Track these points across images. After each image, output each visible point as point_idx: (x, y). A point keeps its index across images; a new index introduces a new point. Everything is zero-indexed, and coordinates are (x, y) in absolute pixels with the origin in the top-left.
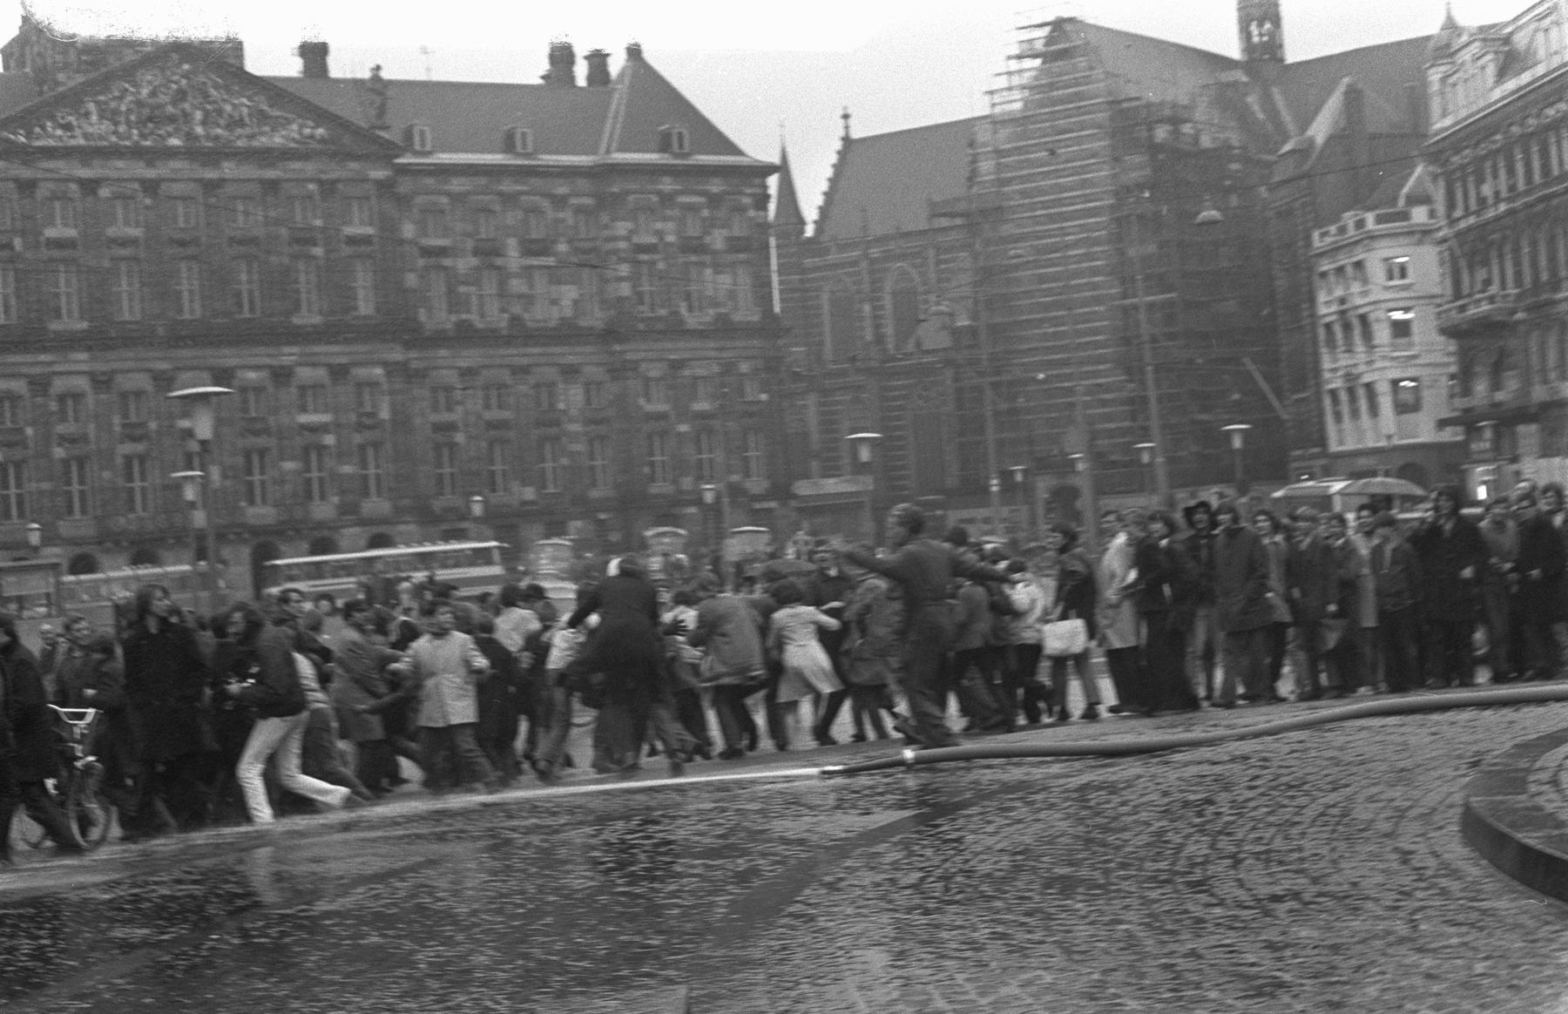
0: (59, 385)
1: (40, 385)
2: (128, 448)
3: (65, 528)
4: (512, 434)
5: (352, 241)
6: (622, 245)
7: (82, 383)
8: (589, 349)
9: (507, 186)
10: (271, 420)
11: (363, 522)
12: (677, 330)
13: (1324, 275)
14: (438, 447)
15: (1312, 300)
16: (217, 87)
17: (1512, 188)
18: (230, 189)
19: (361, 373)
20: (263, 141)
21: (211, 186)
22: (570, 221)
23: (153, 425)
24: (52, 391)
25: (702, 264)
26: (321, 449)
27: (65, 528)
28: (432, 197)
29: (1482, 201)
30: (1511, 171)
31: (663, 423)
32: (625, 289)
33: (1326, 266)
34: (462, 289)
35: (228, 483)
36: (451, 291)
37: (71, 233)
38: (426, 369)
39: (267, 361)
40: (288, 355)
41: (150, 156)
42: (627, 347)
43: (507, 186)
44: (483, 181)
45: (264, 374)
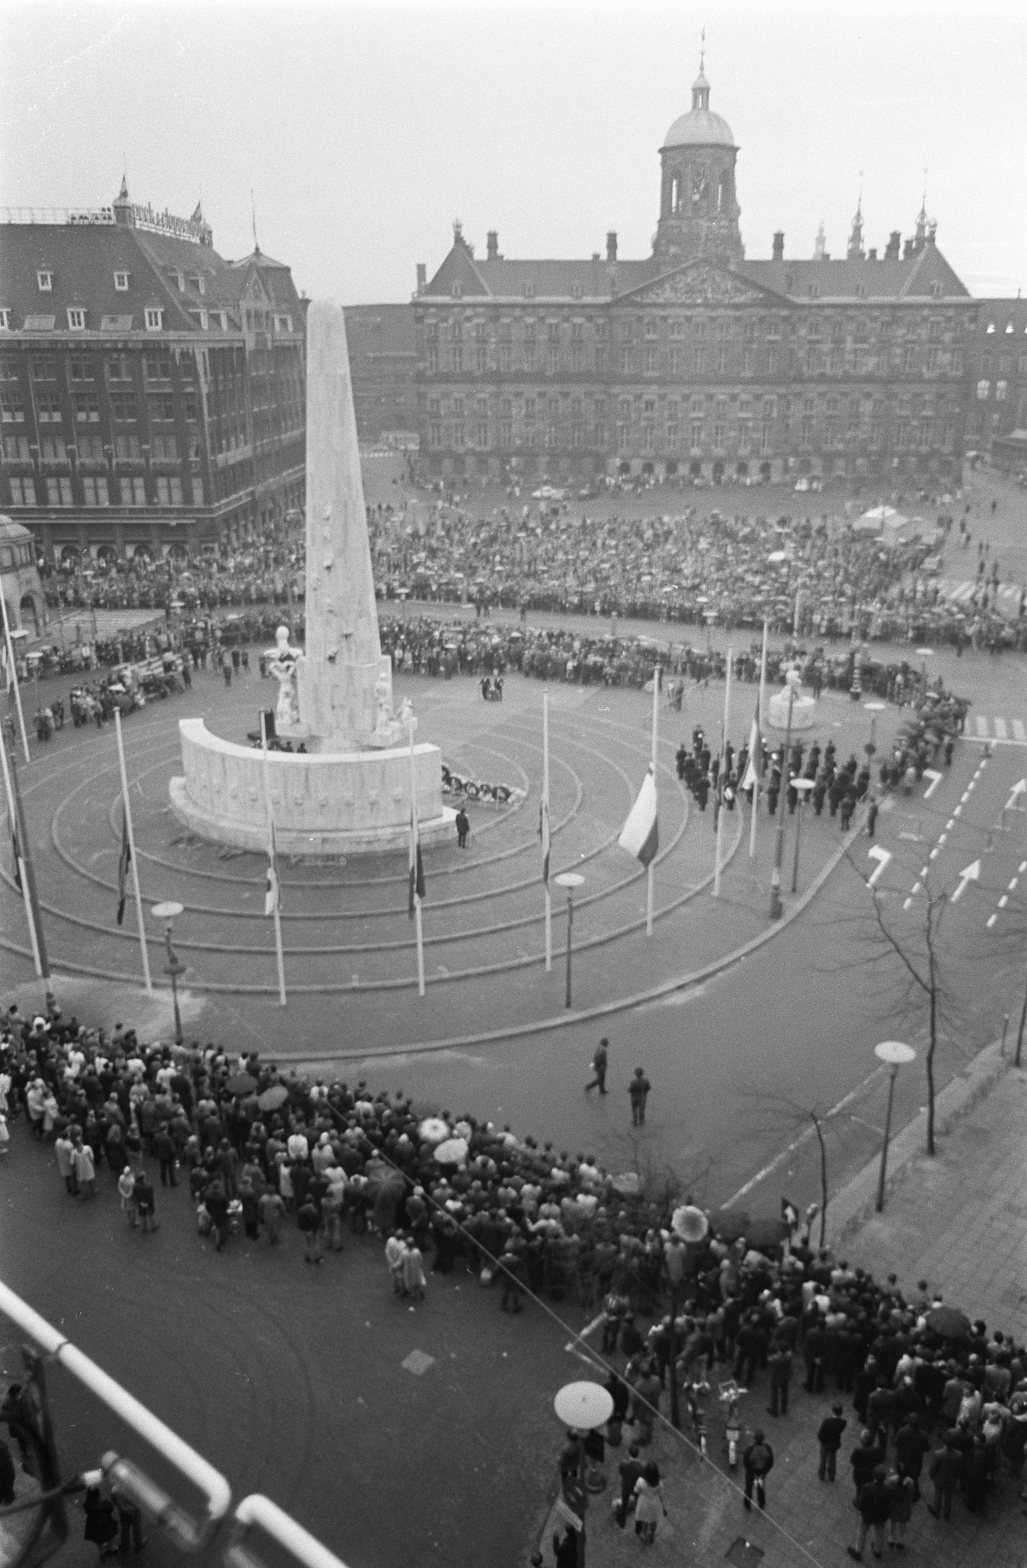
0: (645, 397)
2: (669, 423)
3: (643, 452)
6: (899, 340)
7: (655, 397)
9: (851, 312)
11: (759, 457)
12: (920, 380)
14: (804, 425)
19: (766, 397)
20: (736, 300)
21: (713, 319)
26: (747, 428)
32: (897, 360)
37: (655, 337)
40: (737, 389)
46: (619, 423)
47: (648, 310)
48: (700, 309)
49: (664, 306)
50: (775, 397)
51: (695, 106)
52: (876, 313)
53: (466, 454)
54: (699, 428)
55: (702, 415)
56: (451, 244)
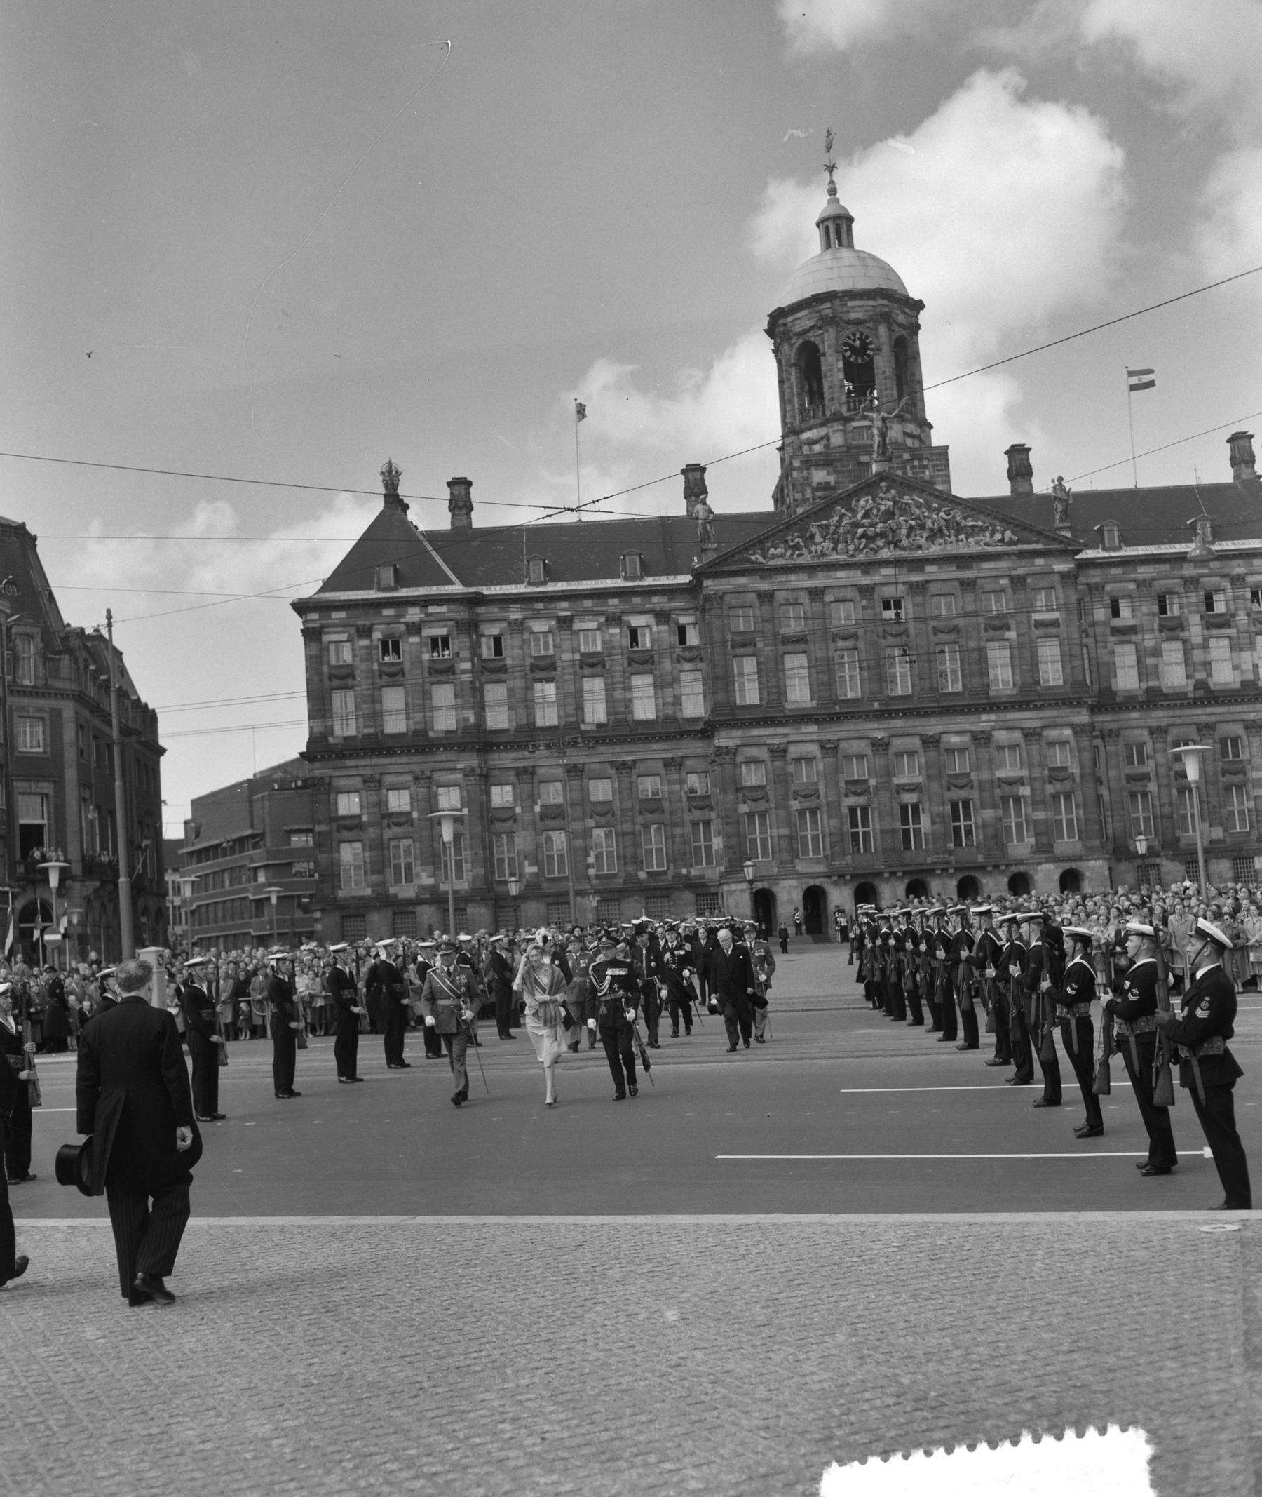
1: (779, 752)
2: (852, 801)
3: (801, 867)
5: (1040, 624)
7: (814, 749)
10: (973, 776)
14: (1133, 795)
16: (919, 506)
18: (933, 588)
19: (1053, 734)
20: (963, 550)
23: (873, 782)
24: (789, 756)
26: (1017, 800)
27: (801, 867)
34: (1150, 661)
35: (936, 827)
38: (1119, 730)
39: (967, 727)
40: (986, 721)
41: (867, 567)
44: (1167, 567)
45: (966, 738)
46: (744, 808)
47: (783, 578)
48: (885, 571)
49: (811, 569)
50: (1068, 732)
51: (828, 245)
52: (1238, 568)
53: (418, 902)
54: (915, 807)
55: (920, 779)
56: (378, 506)
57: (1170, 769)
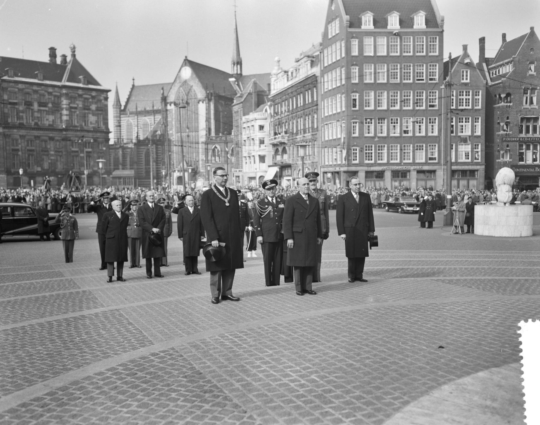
4: (35, 153)
8: (57, 133)
9: (35, 88)
13: (244, 128)
15: (241, 134)
17: (289, 109)
22: (53, 99)
25: (90, 113)
28: (13, 89)
29: (282, 112)
30: (289, 105)
31: (77, 154)
33: (245, 125)
34: (21, 114)
36: (17, 114)
42: (67, 133)
43: (35, 88)
44: (27, 85)
52: (50, 90)
57: (26, 148)
